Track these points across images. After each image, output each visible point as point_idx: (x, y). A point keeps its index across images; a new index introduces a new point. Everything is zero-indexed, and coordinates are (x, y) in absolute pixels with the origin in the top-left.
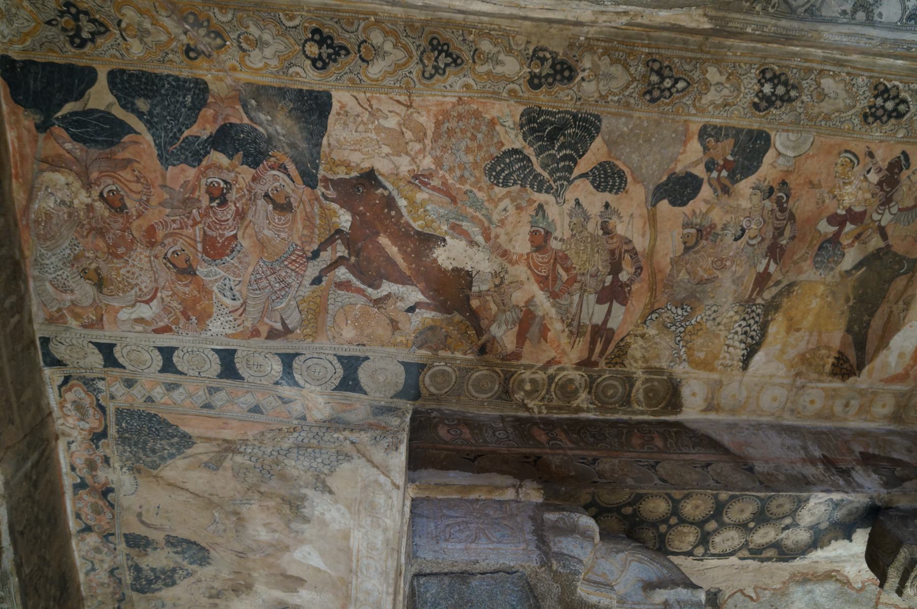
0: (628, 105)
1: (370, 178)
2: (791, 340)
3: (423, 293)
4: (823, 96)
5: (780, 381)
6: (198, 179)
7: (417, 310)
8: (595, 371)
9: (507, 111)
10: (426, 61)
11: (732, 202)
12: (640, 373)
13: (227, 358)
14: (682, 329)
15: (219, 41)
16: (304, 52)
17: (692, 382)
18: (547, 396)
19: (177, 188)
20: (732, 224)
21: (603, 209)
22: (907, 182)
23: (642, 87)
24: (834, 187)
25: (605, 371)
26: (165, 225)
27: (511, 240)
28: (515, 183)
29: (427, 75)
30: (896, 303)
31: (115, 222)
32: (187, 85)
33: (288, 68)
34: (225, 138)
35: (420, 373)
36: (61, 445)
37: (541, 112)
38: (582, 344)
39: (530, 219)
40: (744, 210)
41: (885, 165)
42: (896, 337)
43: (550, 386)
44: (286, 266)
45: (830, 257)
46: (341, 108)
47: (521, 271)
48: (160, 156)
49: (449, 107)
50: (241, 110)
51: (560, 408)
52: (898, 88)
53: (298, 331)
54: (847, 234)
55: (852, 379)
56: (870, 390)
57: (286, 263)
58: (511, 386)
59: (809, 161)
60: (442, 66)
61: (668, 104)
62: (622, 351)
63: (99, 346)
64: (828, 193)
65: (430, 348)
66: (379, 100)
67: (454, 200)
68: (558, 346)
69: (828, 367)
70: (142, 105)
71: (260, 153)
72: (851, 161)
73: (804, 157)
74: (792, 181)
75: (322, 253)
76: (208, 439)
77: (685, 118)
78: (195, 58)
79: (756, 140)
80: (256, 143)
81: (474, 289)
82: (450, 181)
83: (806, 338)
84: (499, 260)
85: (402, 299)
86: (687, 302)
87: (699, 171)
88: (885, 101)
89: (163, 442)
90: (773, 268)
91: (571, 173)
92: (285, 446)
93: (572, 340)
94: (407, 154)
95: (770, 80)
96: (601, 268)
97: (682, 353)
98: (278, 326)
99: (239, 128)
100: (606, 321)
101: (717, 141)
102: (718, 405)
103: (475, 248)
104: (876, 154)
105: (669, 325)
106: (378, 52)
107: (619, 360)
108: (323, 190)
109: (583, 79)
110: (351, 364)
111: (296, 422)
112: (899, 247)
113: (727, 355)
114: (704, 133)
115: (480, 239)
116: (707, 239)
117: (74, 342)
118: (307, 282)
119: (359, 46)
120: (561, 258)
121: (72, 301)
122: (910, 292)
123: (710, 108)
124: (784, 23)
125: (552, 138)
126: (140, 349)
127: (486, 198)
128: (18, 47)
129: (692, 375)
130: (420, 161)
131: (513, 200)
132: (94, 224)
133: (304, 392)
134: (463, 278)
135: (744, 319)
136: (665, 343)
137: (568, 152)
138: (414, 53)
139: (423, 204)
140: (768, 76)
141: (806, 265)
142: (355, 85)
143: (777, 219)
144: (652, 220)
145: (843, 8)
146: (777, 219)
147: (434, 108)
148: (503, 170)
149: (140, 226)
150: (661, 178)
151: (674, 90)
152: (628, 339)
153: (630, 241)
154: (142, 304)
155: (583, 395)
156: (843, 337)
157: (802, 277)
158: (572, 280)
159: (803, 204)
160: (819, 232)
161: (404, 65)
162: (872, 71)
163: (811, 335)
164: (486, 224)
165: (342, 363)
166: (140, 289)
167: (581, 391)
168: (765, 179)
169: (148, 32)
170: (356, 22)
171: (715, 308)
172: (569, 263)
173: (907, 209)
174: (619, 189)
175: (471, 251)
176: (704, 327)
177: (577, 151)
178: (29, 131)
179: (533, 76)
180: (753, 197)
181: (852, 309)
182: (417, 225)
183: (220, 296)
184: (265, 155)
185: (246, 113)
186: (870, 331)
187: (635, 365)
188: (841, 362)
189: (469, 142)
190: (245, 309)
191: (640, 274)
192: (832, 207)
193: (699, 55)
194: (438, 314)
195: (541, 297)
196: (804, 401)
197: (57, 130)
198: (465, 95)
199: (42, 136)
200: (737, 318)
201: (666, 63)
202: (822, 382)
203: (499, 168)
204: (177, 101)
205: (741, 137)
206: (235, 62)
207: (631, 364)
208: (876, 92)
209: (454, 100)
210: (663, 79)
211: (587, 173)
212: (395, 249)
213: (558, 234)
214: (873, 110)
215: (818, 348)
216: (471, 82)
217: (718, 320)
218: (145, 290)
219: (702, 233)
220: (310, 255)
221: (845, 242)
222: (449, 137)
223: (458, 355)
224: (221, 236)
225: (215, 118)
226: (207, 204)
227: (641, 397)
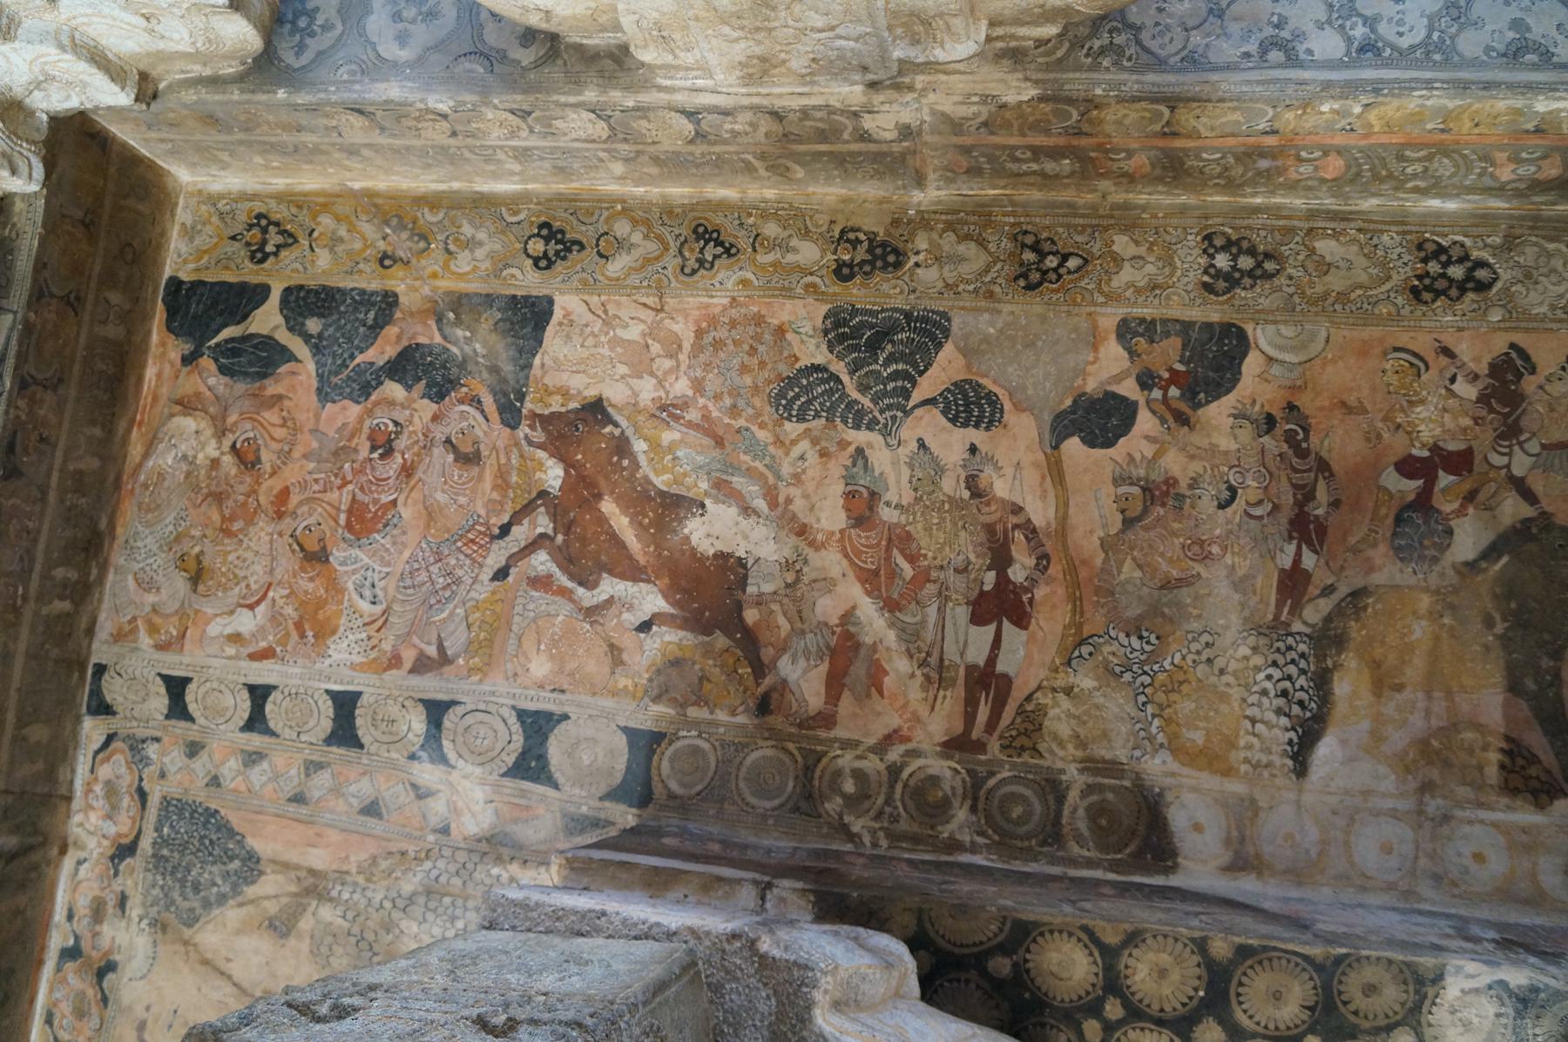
0: (990, 295)
1: (596, 410)
2: (1389, 709)
3: (665, 597)
4: (1325, 267)
5: (1389, 804)
6: (361, 421)
7: (655, 628)
8: (981, 763)
9: (802, 312)
10: (687, 254)
11: (1196, 439)
13: (345, 704)
14: (1147, 680)
15: (422, 244)
17: (1188, 797)
18: (888, 809)
19: (331, 433)
20: (1207, 477)
21: (967, 455)
23: (1013, 269)
24: (1392, 409)
25: (1001, 763)
27: (812, 508)
28: (817, 416)
29: (687, 270)
33: (501, 270)
34: (406, 365)
35: (654, 752)
36: (68, 863)
37: (855, 311)
38: (951, 703)
40: (1226, 453)
41: (1483, 369)
43: (892, 787)
44: (459, 549)
47: (831, 561)
48: (319, 390)
49: (717, 310)
50: (434, 327)
51: (915, 839)
52: (1463, 246)
53: (461, 661)
54: (1444, 491)
58: (816, 783)
59: (1329, 369)
61: (1058, 291)
62: (1031, 725)
64: (1385, 419)
65: (673, 701)
66: (618, 304)
67: (719, 442)
68: (905, 706)
69: (1492, 774)
71: (451, 382)
73: (1318, 362)
74: (1304, 402)
75: (514, 529)
76: (286, 866)
77: (1088, 309)
80: (445, 368)
81: (751, 589)
82: (715, 414)
83: (1420, 705)
85: (631, 608)
86: (1146, 624)
87: (1129, 389)
88: (1445, 265)
89: (215, 869)
90: (1309, 560)
91: (907, 398)
92: (407, 888)
94: (652, 374)
95: (1224, 248)
96: (972, 557)
97: (1154, 730)
98: (432, 651)
100: (992, 660)
102: (1258, 856)
103: (752, 520)
104: (1456, 351)
105: (1118, 669)
106: (621, 244)
108: (527, 430)
109: (917, 265)
110: (538, 725)
111: (431, 838)
113: (1255, 740)
114: (1125, 331)
115: (761, 504)
116: (1163, 505)
123: (1129, 293)
124: (1150, 77)
125: (874, 346)
126: (222, 687)
128: (192, 266)
129: (1184, 780)
131: (815, 442)
132: (213, 488)
133: (455, 775)
134: (730, 571)
135: (1275, 664)
136: (1116, 706)
137: (900, 367)
138: (672, 244)
139: (671, 449)
140: (1218, 242)
141: (1380, 553)
142: (588, 286)
143: (1296, 471)
144: (1055, 471)
145: (1243, 49)
146: (1296, 471)
148: (797, 397)
149: (271, 488)
150: (1061, 402)
151: (1062, 271)
152: (1043, 699)
153: (1021, 509)
154: (245, 610)
155: (961, 814)
156: (1506, 705)
158: (922, 577)
159: (1339, 442)
161: (657, 259)
162: (1403, 223)
163: (1429, 695)
164: (771, 480)
165: (523, 723)
166: (248, 586)
167: (956, 803)
168: (1254, 401)
169: (342, 240)
170: (597, 212)
171: (1206, 638)
172: (914, 545)
174: (991, 422)
175: (745, 524)
176: (1190, 676)
177: (915, 365)
178: (172, 365)
179: (841, 265)
180: (1238, 431)
181: (1504, 639)
182: (661, 481)
183: (355, 597)
184: (453, 383)
187: (1061, 753)
188: (1520, 761)
191: (1046, 568)
192: (1398, 445)
193: (1094, 222)
194: (689, 635)
195: (869, 612)
196: (1459, 855)
197: (207, 362)
199: (185, 370)
200: (1258, 660)
201: (1045, 235)
202: (1490, 808)
203: (791, 394)
205: (1195, 336)
206: (436, 267)
207: (1052, 752)
208: (1423, 254)
209: (725, 301)
210: (1042, 255)
212: (625, 521)
213: (891, 496)
214: (1427, 281)
215: (1455, 727)
216: (750, 276)
217: (1220, 663)
218: (254, 587)
219: (1155, 496)
220: (497, 531)
223: (722, 716)
224: (375, 502)
225: (399, 338)
227: (1082, 826)
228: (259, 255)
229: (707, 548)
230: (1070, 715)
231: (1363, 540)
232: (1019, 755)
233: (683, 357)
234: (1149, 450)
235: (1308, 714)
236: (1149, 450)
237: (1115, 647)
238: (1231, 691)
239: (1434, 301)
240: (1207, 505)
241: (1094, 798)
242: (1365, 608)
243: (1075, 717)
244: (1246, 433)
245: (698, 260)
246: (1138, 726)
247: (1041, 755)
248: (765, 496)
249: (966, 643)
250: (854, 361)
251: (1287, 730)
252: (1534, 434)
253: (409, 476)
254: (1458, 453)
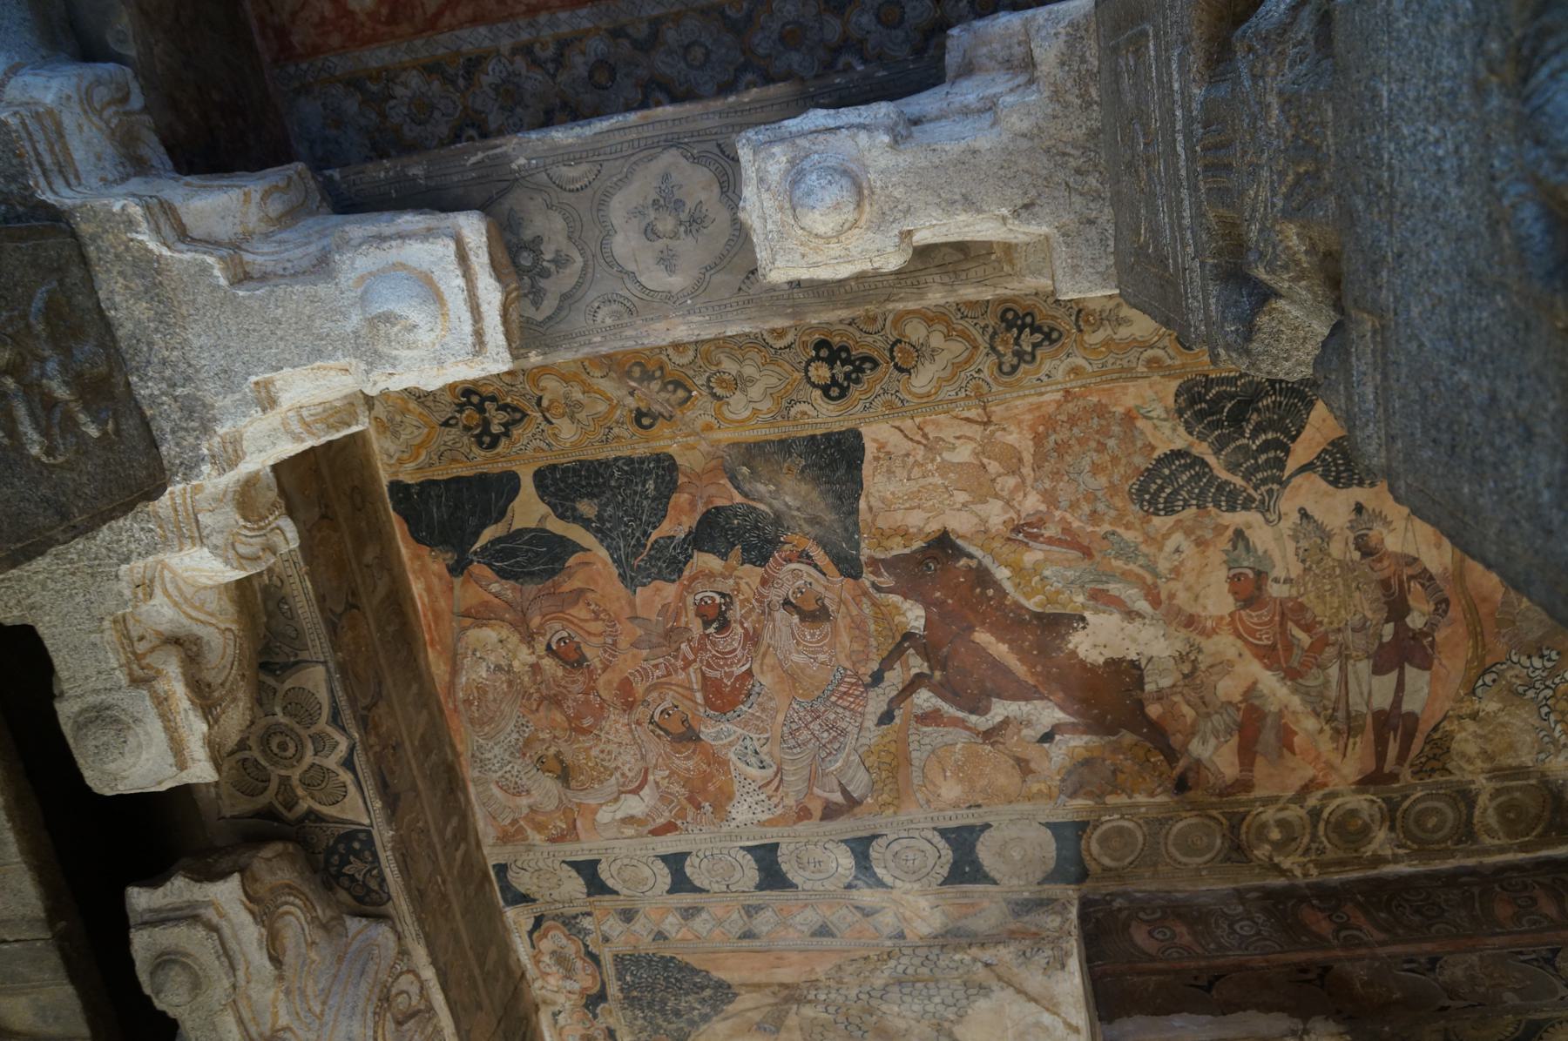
1: (943, 545)
3: (1062, 708)
6: (682, 598)
7: (1057, 737)
8: (1395, 790)
9: (1149, 393)
10: (1000, 348)
12: (1482, 780)
14: (1549, 692)
15: (681, 393)
16: (808, 378)
18: (1314, 846)
19: (654, 617)
21: (1353, 516)
25: (1414, 787)
26: (645, 674)
27: (1197, 598)
28: (1186, 505)
29: (1006, 368)
31: (574, 682)
32: (645, 466)
33: (788, 409)
34: (713, 531)
35: (1080, 838)
36: (544, 1020)
37: (1209, 383)
39: (1225, 557)
43: (1315, 826)
46: (879, 450)
47: (1225, 645)
48: (622, 577)
49: (1052, 409)
50: (729, 485)
51: (1341, 863)
53: (869, 800)
57: (833, 699)
58: (1243, 837)
60: (1029, 349)
62: (1439, 750)
63: (575, 865)
65: (1089, 795)
66: (937, 424)
67: (1087, 553)
68: (1318, 757)
70: (587, 508)
71: (768, 541)
75: (887, 675)
76: (757, 987)
78: (651, 426)
80: (758, 528)
81: (1148, 688)
82: (1076, 524)
84: (1183, 633)
85: (1029, 724)
89: (689, 998)
91: (1282, 469)
92: (879, 982)
93: (1342, 743)
94: (997, 496)
96: (1369, 614)
97: (1557, 734)
98: (837, 797)
99: (731, 511)
103: (1138, 622)
105: (1521, 689)
106: (921, 352)
107: (1437, 765)
108: (873, 578)
110: (962, 840)
111: (889, 943)
115: (1143, 605)
117: (541, 864)
118: (870, 722)
119: (891, 351)
120: (1291, 610)
121: (530, 807)
125: (1237, 419)
126: (634, 862)
127: (1140, 539)
128: (410, 466)
130: (1020, 503)
131: (1188, 533)
132: (545, 692)
133: (896, 894)
134: (1124, 676)
137: (1270, 436)
138: (979, 339)
142: (896, 408)
147: (1028, 417)
148: (1161, 488)
149: (609, 682)
152: (1447, 726)
153: (1416, 560)
158: (1321, 643)
161: (967, 361)
164: (1149, 579)
165: (948, 840)
166: (623, 775)
167: (1375, 827)
169: (580, 404)
172: (1308, 615)
175: (1131, 628)
177: (1286, 431)
178: (440, 578)
182: (1033, 604)
184: (775, 543)
185: (737, 488)
187: (1471, 768)
189: (1095, 456)
190: (781, 780)
191: (1446, 612)
194: (1095, 738)
197: (478, 569)
198: (1075, 385)
199: (458, 581)
203: (1154, 487)
204: (636, 493)
206: (708, 418)
207: (1461, 768)
209: (1058, 396)
211: (1311, 463)
213: (1279, 572)
220: (868, 679)
222: (1061, 456)
223: (1141, 798)
225: (692, 504)
226: (701, 631)
227: (1493, 820)
228: (488, 439)
229: (1096, 657)
233: (1026, 470)
237: (1517, 670)
243: (1481, 737)
245: (1016, 353)
247: (1451, 773)
248: (1146, 597)
249: (1370, 694)
250: (1218, 438)
253: (756, 644)
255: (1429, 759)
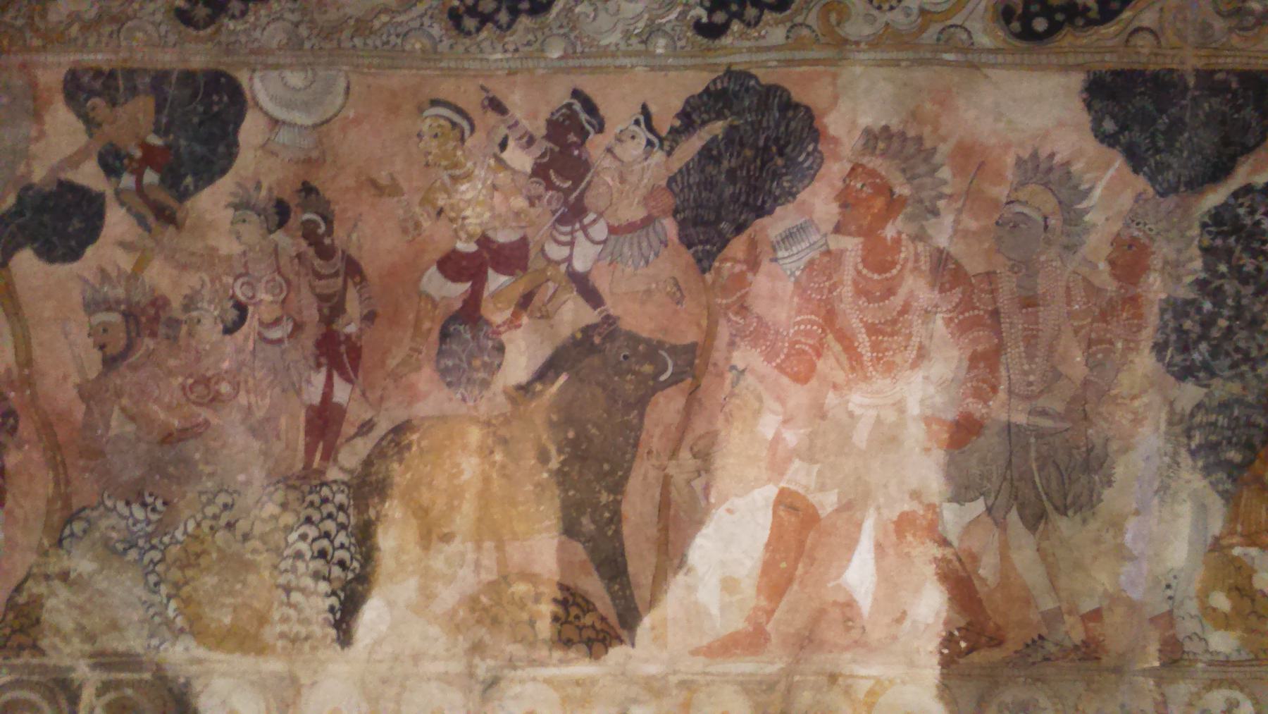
2: (438, 563)
5: (440, 667)
14: (156, 555)
20: (206, 293)
22: (608, 162)
24: (430, 189)
30: (674, 454)
40: (229, 258)
41: (539, 128)
42: (699, 540)
45: (471, 356)
54: (495, 295)
55: (616, 653)
56: (673, 679)
64: (421, 204)
69: (545, 628)
72: (454, 124)
77: (20, 58)
79: (208, 95)
87: (89, 175)
90: (342, 392)
101: (113, 103)
104: (507, 104)
105: (120, 547)
107: (22, 638)
112: (639, 320)
113: (292, 612)
116: (153, 335)
122: (699, 426)
135: (309, 520)
136: (123, 591)
141: (425, 378)
146: (320, 277)
156: (561, 548)
157: (424, 409)
159: (372, 235)
160: (429, 297)
163: (479, 548)
168: (258, 186)
171: (222, 499)
173: (631, 227)
180: (241, 228)
181: (561, 477)
186: (626, 530)
187: (68, 650)
188: (574, 611)
192: (440, 237)
200: (288, 518)
202: (543, 664)
207: (55, 647)
215: (505, 579)
217: (242, 526)
219: (141, 323)
221: (497, 315)
230: (70, 605)
231: (404, 363)
232: (18, 656)
234: (126, 262)
235: (350, 576)
236: (126, 262)
237: (113, 520)
238: (259, 558)
239: (478, 30)
240: (209, 331)
241: (111, 696)
242: (409, 447)
244: (252, 230)
246: (152, 611)
247: (42, 653)
251: (328, 596)
252: (601, 215)
254: (512, 246)
255: (14, 632)
